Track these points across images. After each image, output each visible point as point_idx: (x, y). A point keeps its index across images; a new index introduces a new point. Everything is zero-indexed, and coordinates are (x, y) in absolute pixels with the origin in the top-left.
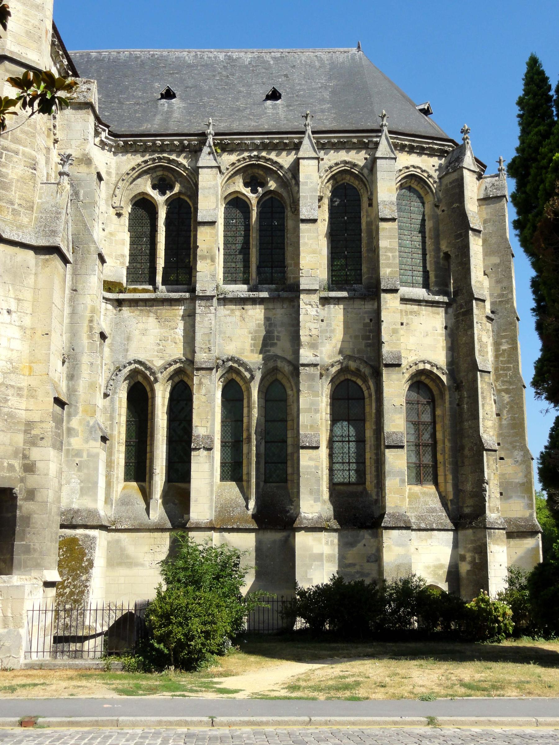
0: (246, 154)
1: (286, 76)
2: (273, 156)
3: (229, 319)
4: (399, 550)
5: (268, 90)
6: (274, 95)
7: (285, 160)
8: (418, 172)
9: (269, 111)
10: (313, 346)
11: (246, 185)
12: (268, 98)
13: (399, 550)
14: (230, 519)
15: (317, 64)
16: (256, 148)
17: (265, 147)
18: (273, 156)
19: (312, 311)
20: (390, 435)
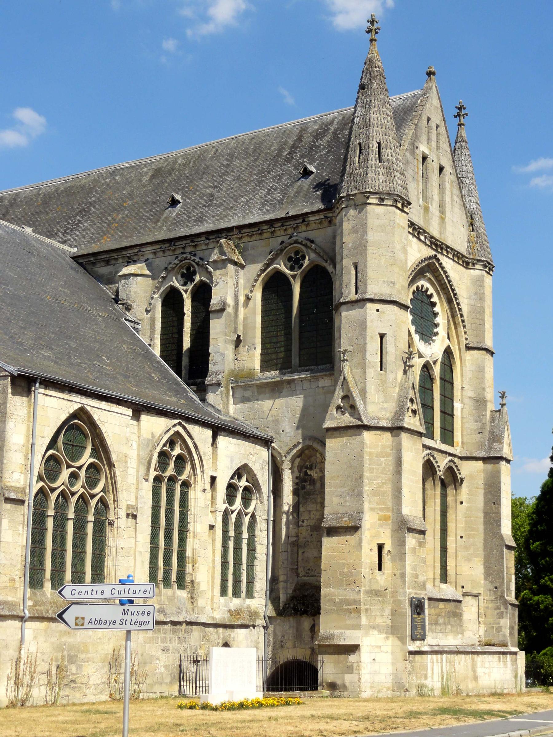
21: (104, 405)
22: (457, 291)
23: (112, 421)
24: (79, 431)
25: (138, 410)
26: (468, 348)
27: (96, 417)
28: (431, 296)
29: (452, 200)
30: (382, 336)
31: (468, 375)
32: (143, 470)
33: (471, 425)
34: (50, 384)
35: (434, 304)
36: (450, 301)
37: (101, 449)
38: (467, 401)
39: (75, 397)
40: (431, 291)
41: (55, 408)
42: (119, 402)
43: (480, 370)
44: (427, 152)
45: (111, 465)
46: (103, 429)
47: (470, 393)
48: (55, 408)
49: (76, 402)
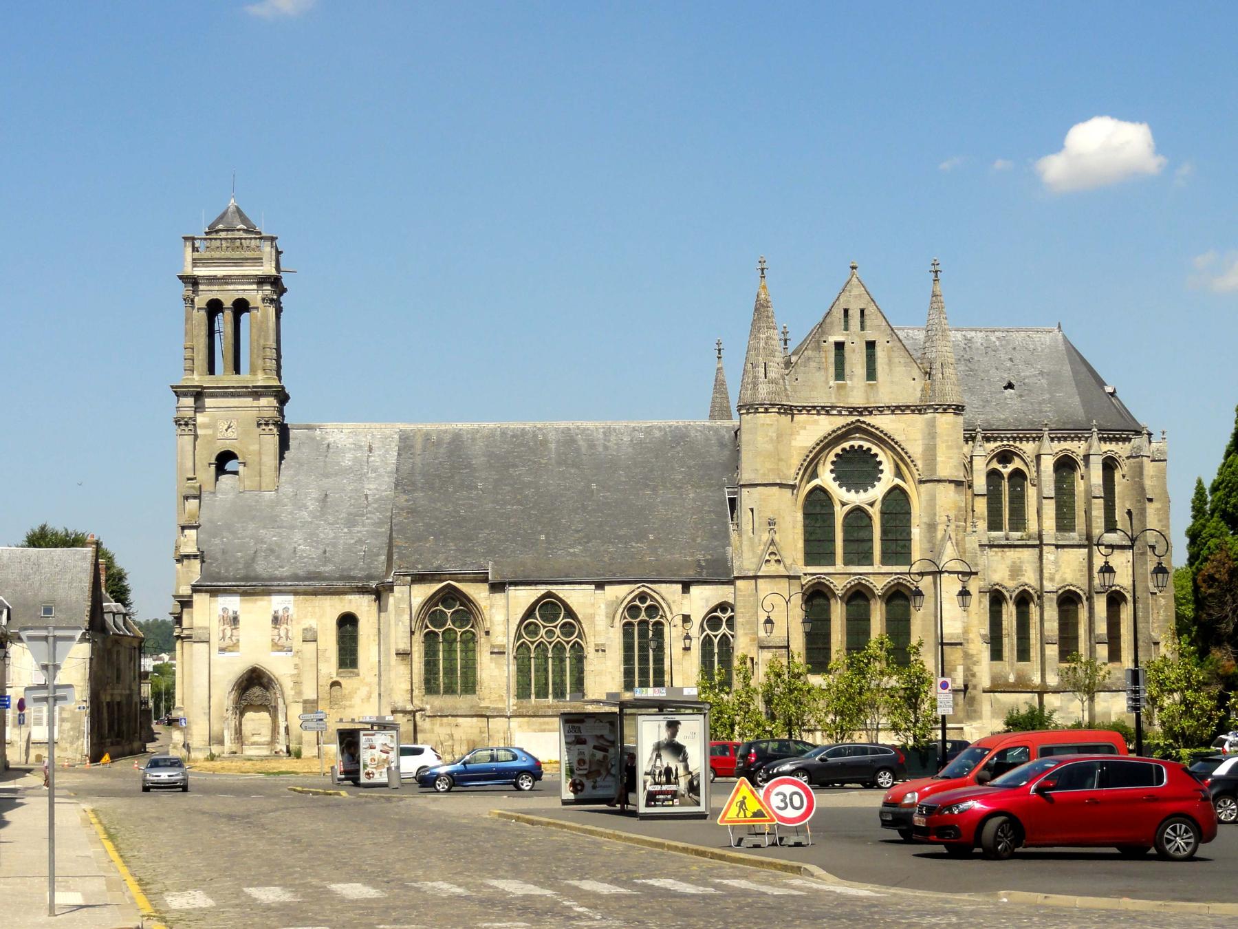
0: (999, 443)
1: (1011, 360)
2: (1017, 444)
3: (995, 558)
4: (1105, 704)
5: (1005, 384)
6: (1010, 386)
7: (1028, 448)
8: (1112, 454)
9: (1009, 401)
10: (1052, 580)
11: (999, 462)
12: (1006, 388)
13: (1105, 704)
14: (998, 685)
15: (1031, 347)
16: (1008, 440)
17: (1014, 439)
18: (1017, 444)
19: (1052, 557)
20: (1099, 635)
21: (567, 587)
22: (897, 438)
23: (577, 597)
24: (549, 607)
25: (600, 585)
26: (921, 482)
27: (561, 595)
28: (869, 449)
29: (890, 362)
30: (752, 510)
31: (924, 504)
32: (609, 622)
33: (926, 546)
34: (516, 584)
35: (876, 455)
36: (893, 449)
37: (570, 613)
38: (923, 526)
39: (539, 587)
40: (866, 445)
41: (524, 597)
42: (580, 583)
43: (932, 500)
44: (840, 339)
45: (580, 622)
46: (568, 601)
47: (925, 520)
48: (524, 597)
49: (542, 590)
